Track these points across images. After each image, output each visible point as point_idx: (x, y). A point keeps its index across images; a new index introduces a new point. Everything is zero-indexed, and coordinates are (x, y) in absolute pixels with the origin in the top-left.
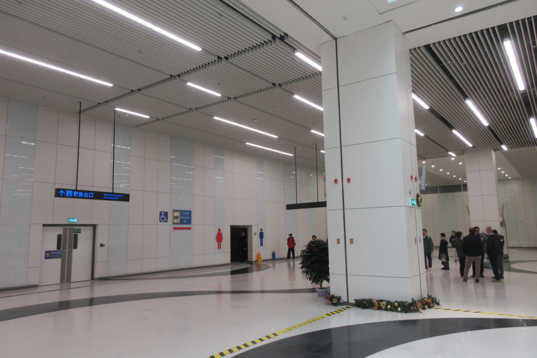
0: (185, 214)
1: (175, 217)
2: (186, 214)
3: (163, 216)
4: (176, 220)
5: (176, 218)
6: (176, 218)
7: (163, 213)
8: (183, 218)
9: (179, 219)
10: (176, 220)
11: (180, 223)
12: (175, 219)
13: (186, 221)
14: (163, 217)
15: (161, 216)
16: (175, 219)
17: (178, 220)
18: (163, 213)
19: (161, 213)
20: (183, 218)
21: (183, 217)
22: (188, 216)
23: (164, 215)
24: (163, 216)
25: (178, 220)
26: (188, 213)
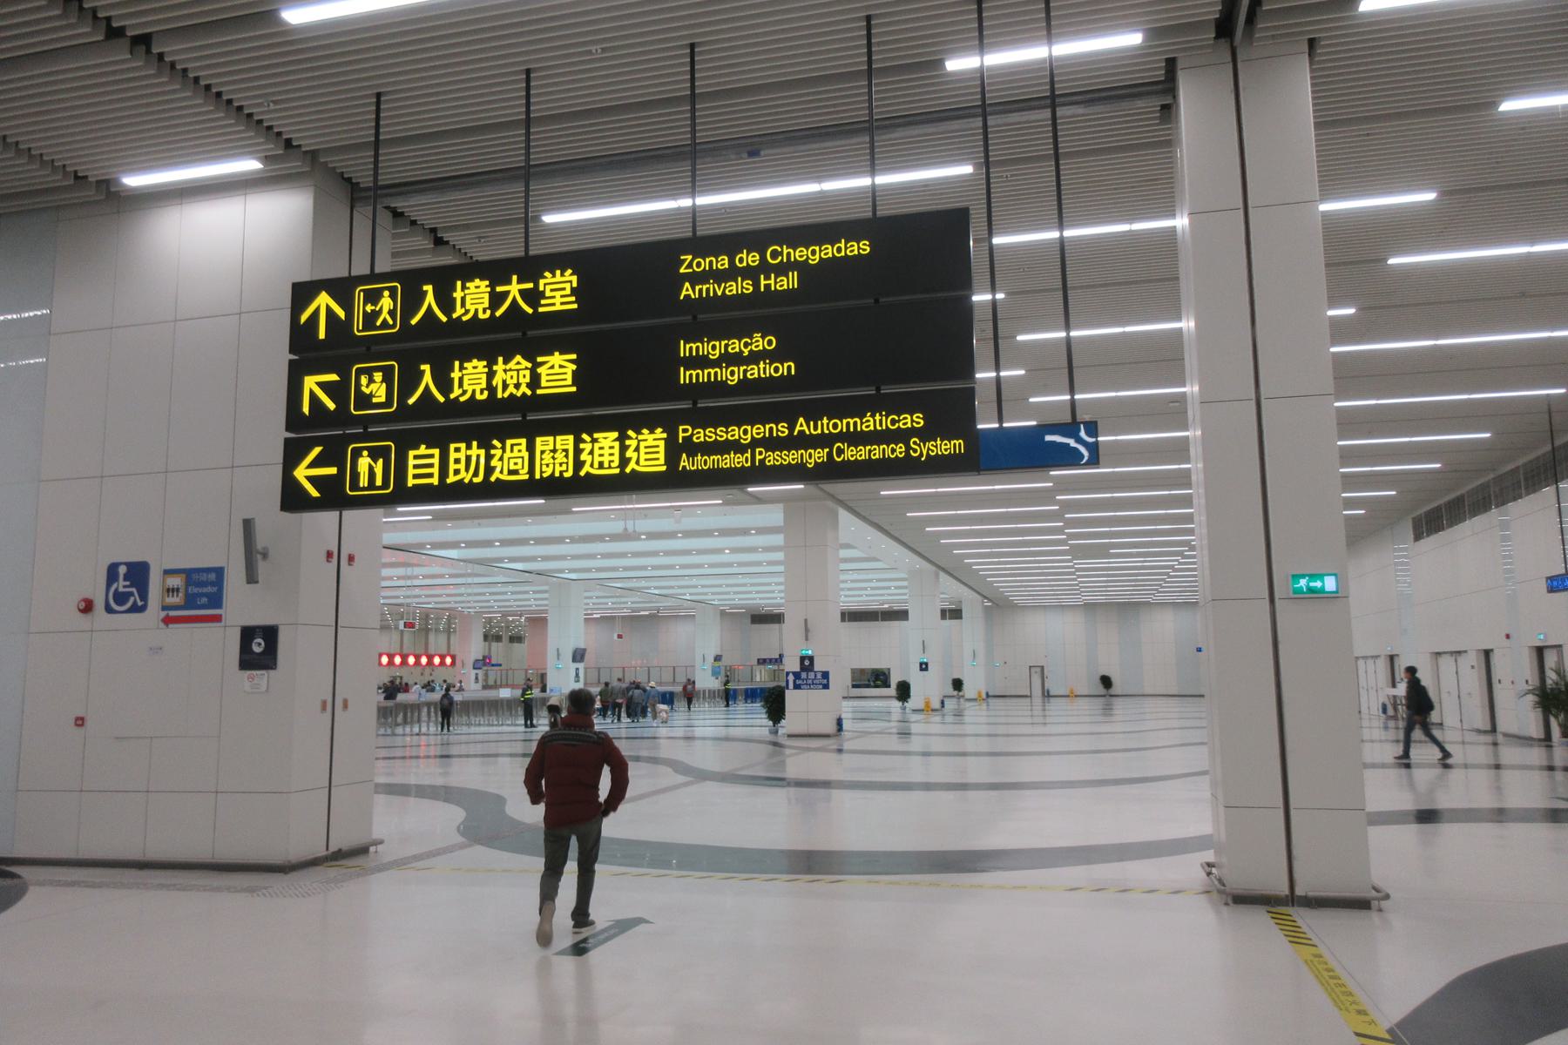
0: (204, 577)
1: (171, 591)
2: (205, 579)
3: (121, 585)
4: (173, 596)
5: (173, 591)
6: (173, 591)
7: (122, 570)
8: (196, 590)
9: (180, 595)
10: (173, 596)
11: (183, 603)
12: (171, 594)
13: (204, 600)
14: (121, 589)
15: (115, 586)
16: (171, 594)
17: (177, 596)
18: (122, 570)
19: (112, 571)
20: (196, 590)
21: (196, 587)
22: (212, 584)
23: (125, 580)
24: (122, 583)
25: (177, 596)
26: (212, 576)
